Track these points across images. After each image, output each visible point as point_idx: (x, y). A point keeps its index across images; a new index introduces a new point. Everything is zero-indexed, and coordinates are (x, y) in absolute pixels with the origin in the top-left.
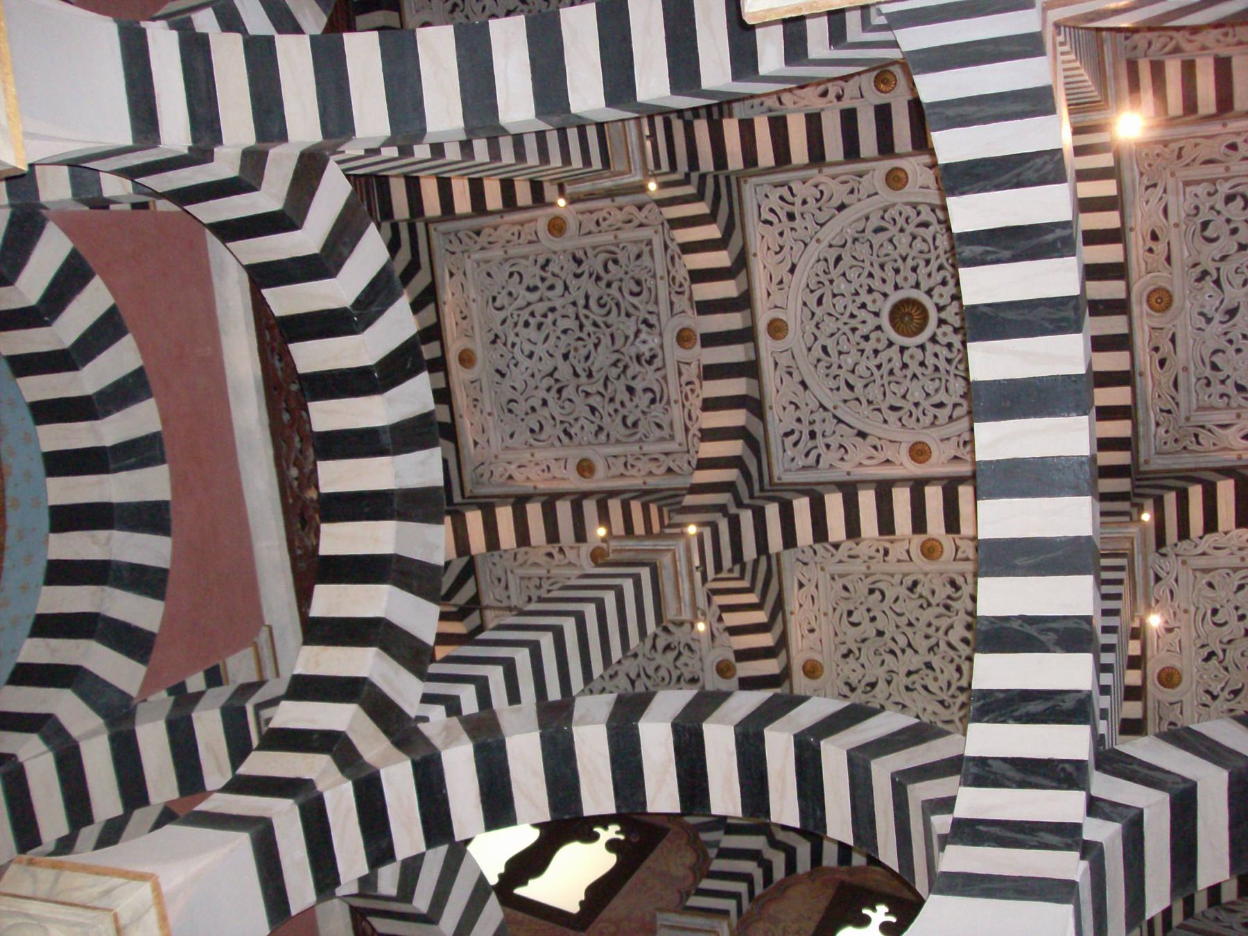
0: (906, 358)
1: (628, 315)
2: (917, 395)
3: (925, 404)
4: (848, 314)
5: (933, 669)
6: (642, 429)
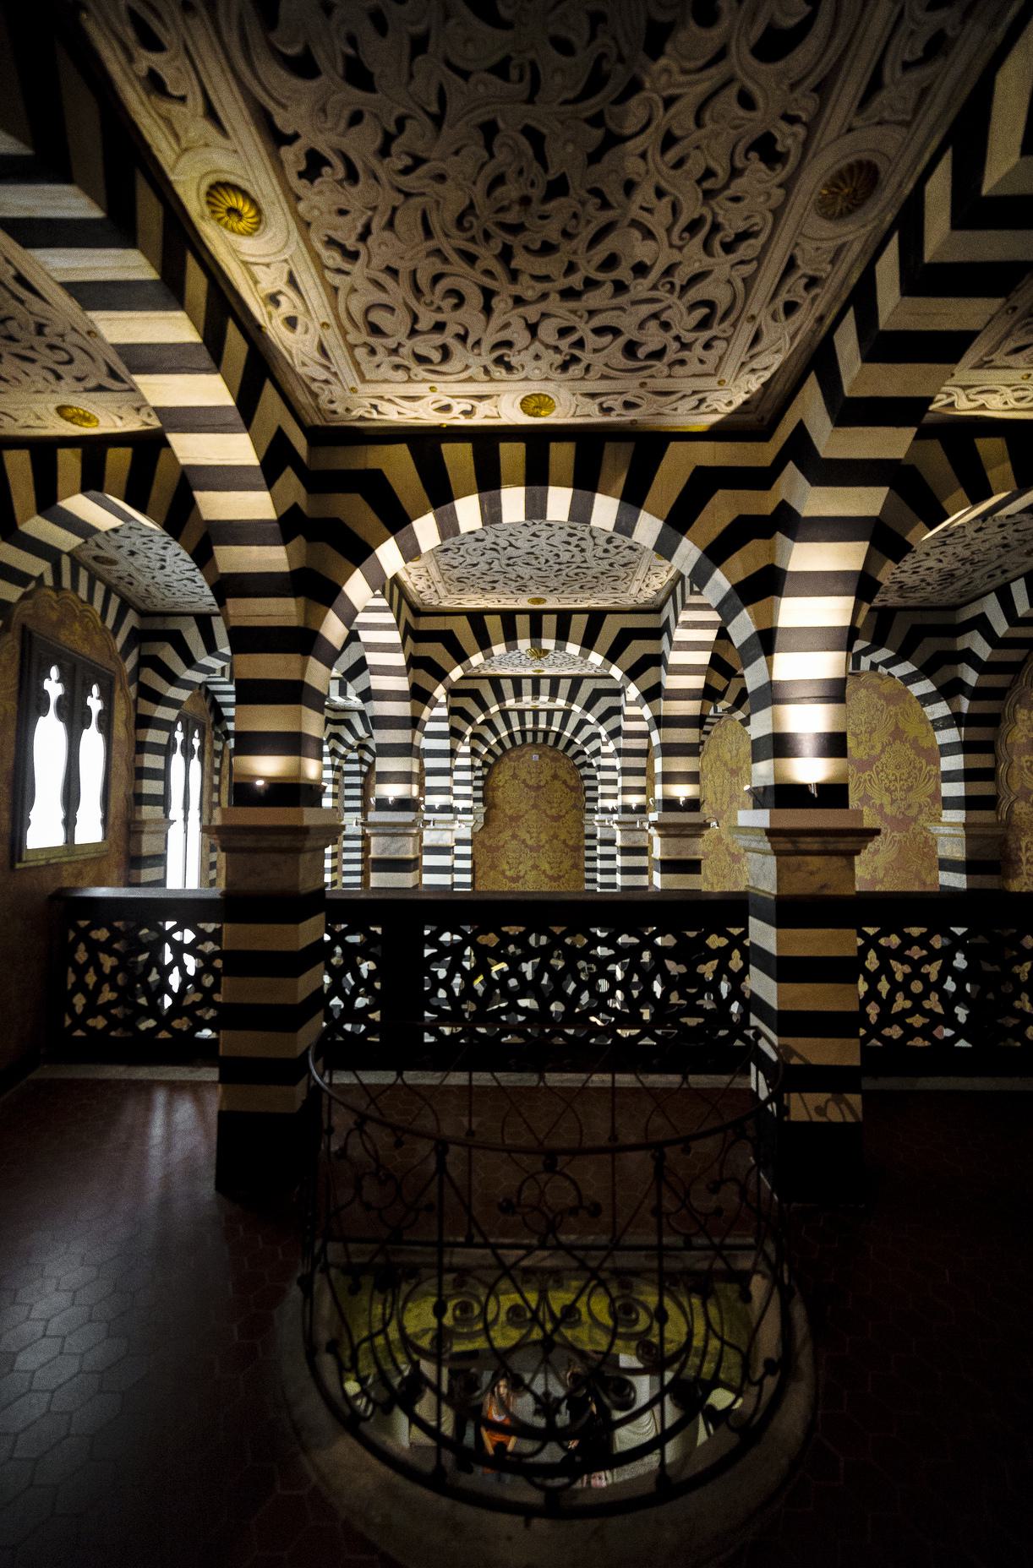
5: (547, 198)
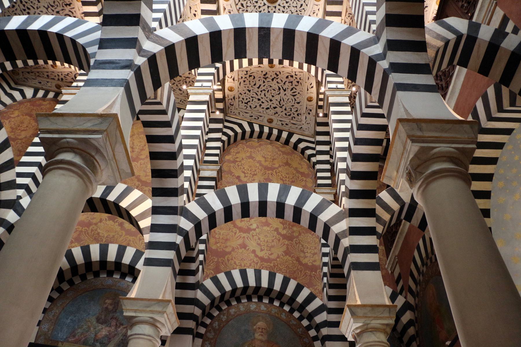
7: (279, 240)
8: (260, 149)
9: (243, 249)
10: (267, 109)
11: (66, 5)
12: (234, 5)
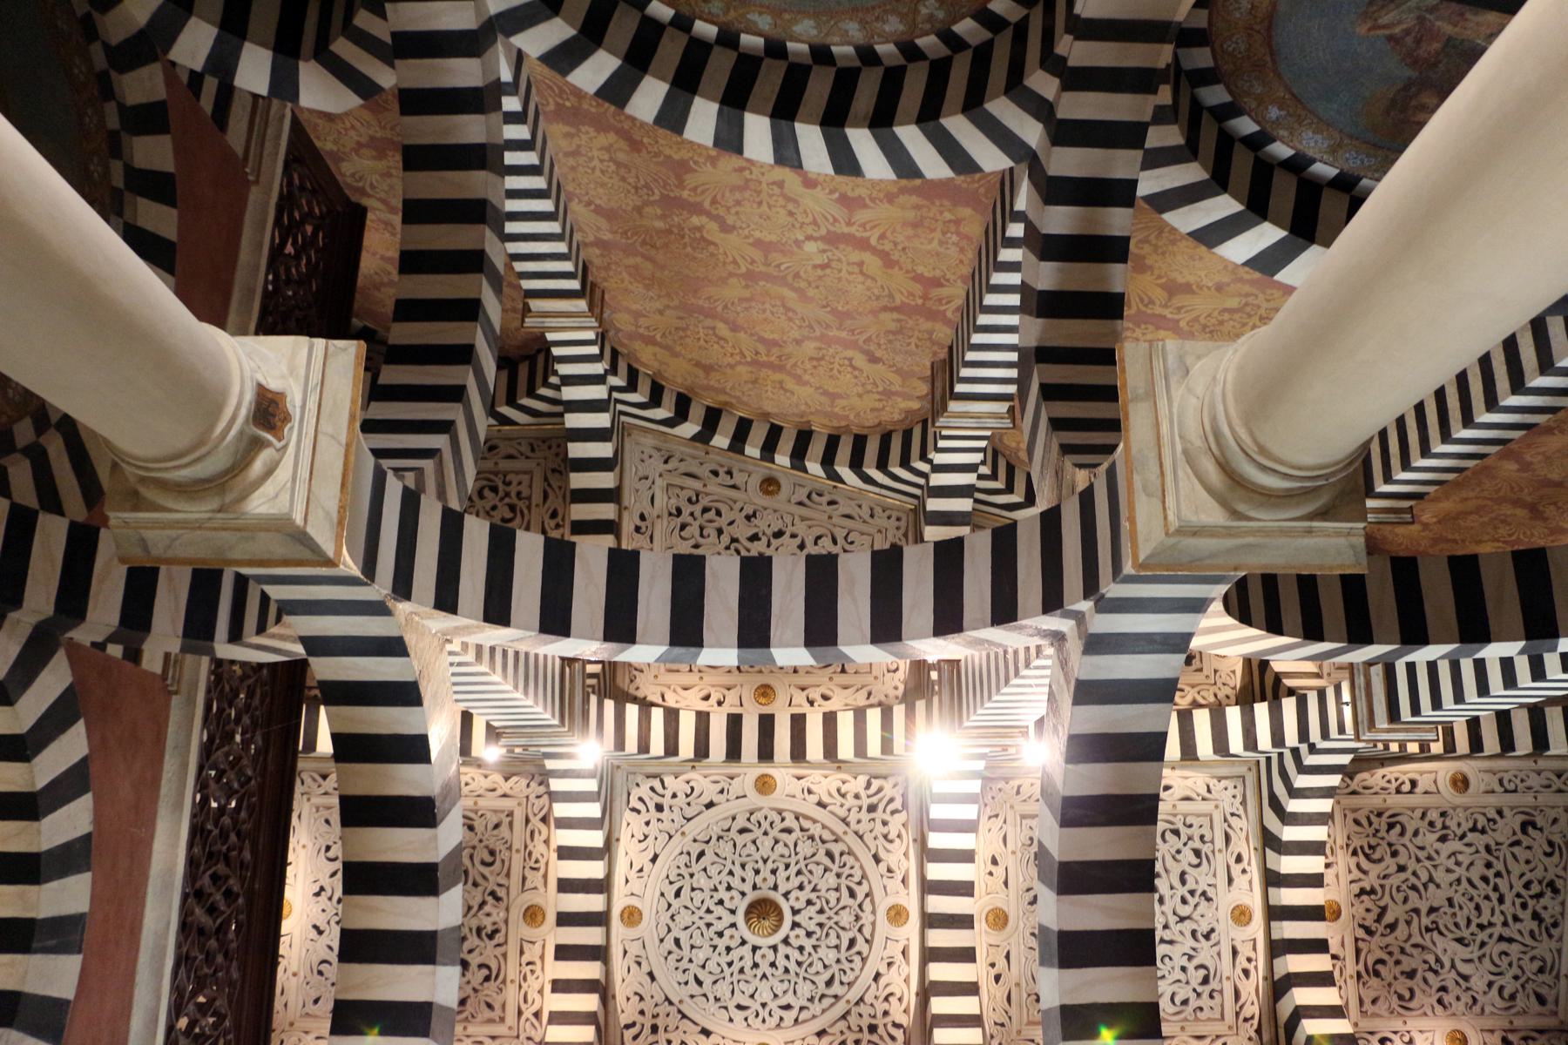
0: (758, 958)
1: (475, 884)
2: (766, 996)
3: (773, 1005)
4: (704, 908)
6: (469, 1007)
7: (714, 202)
8: (803, 408)
9: (850, 194)
10: (779, 534)
11: (1373, 891)
12: (878, 893)
